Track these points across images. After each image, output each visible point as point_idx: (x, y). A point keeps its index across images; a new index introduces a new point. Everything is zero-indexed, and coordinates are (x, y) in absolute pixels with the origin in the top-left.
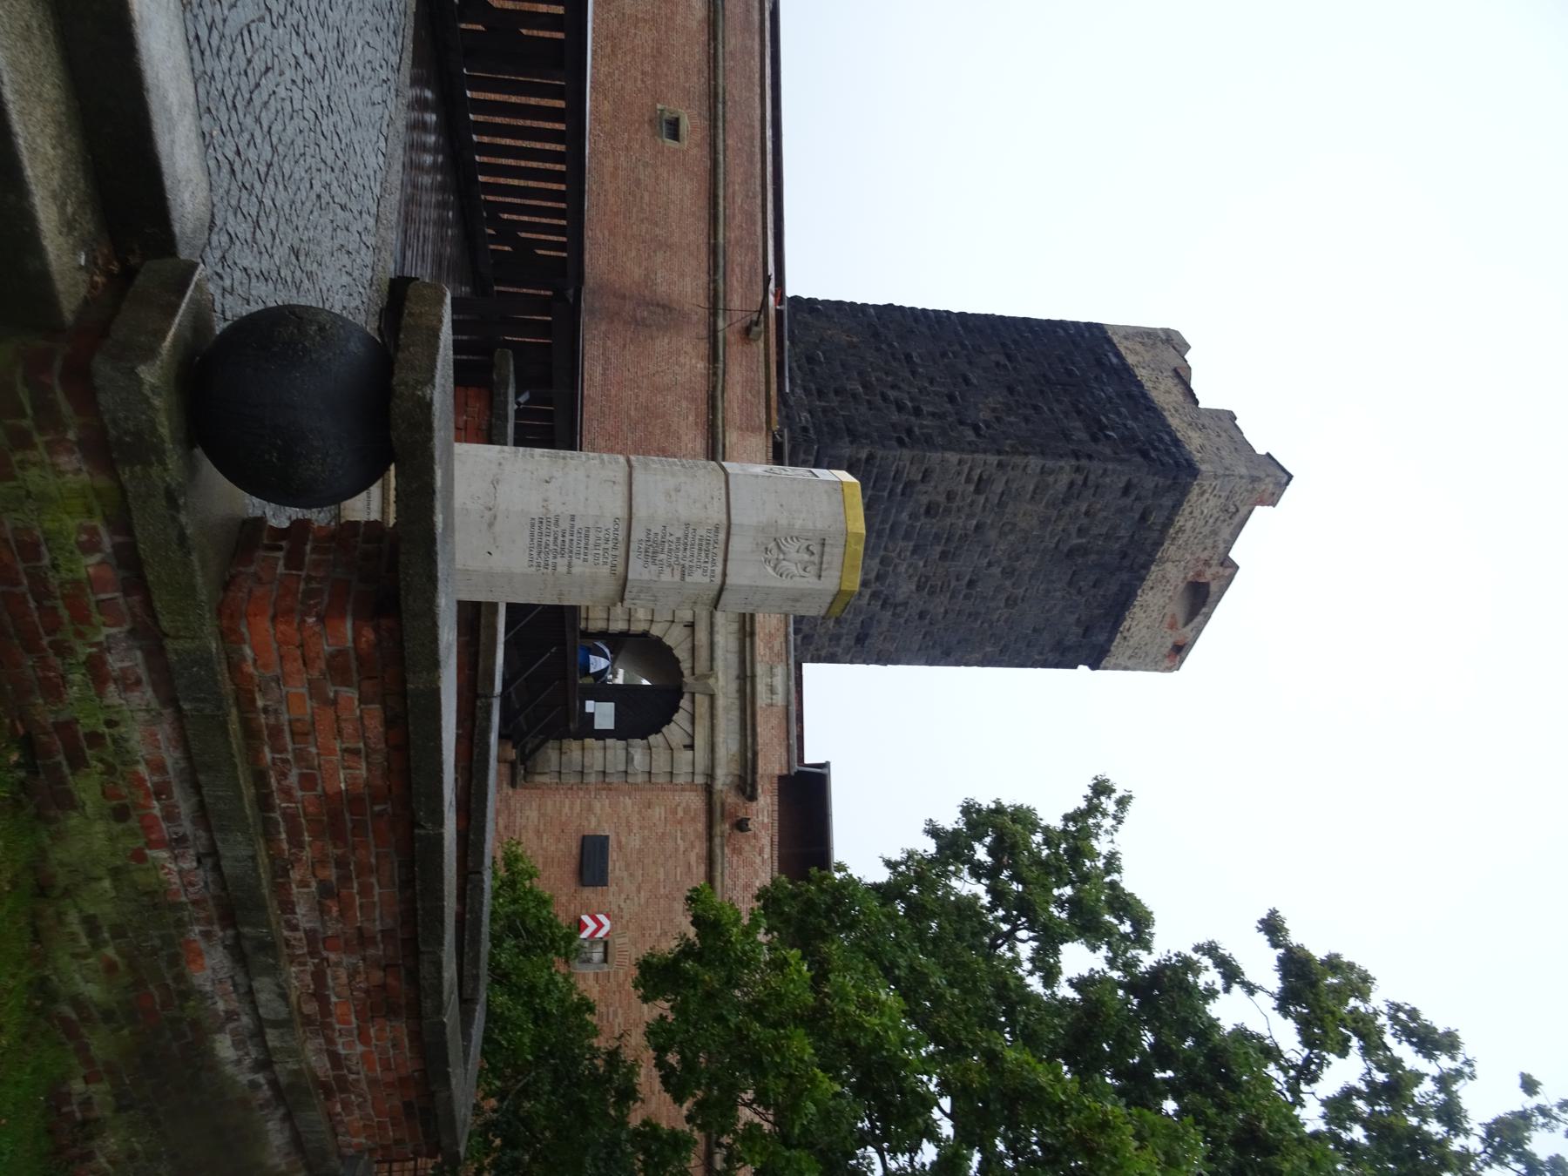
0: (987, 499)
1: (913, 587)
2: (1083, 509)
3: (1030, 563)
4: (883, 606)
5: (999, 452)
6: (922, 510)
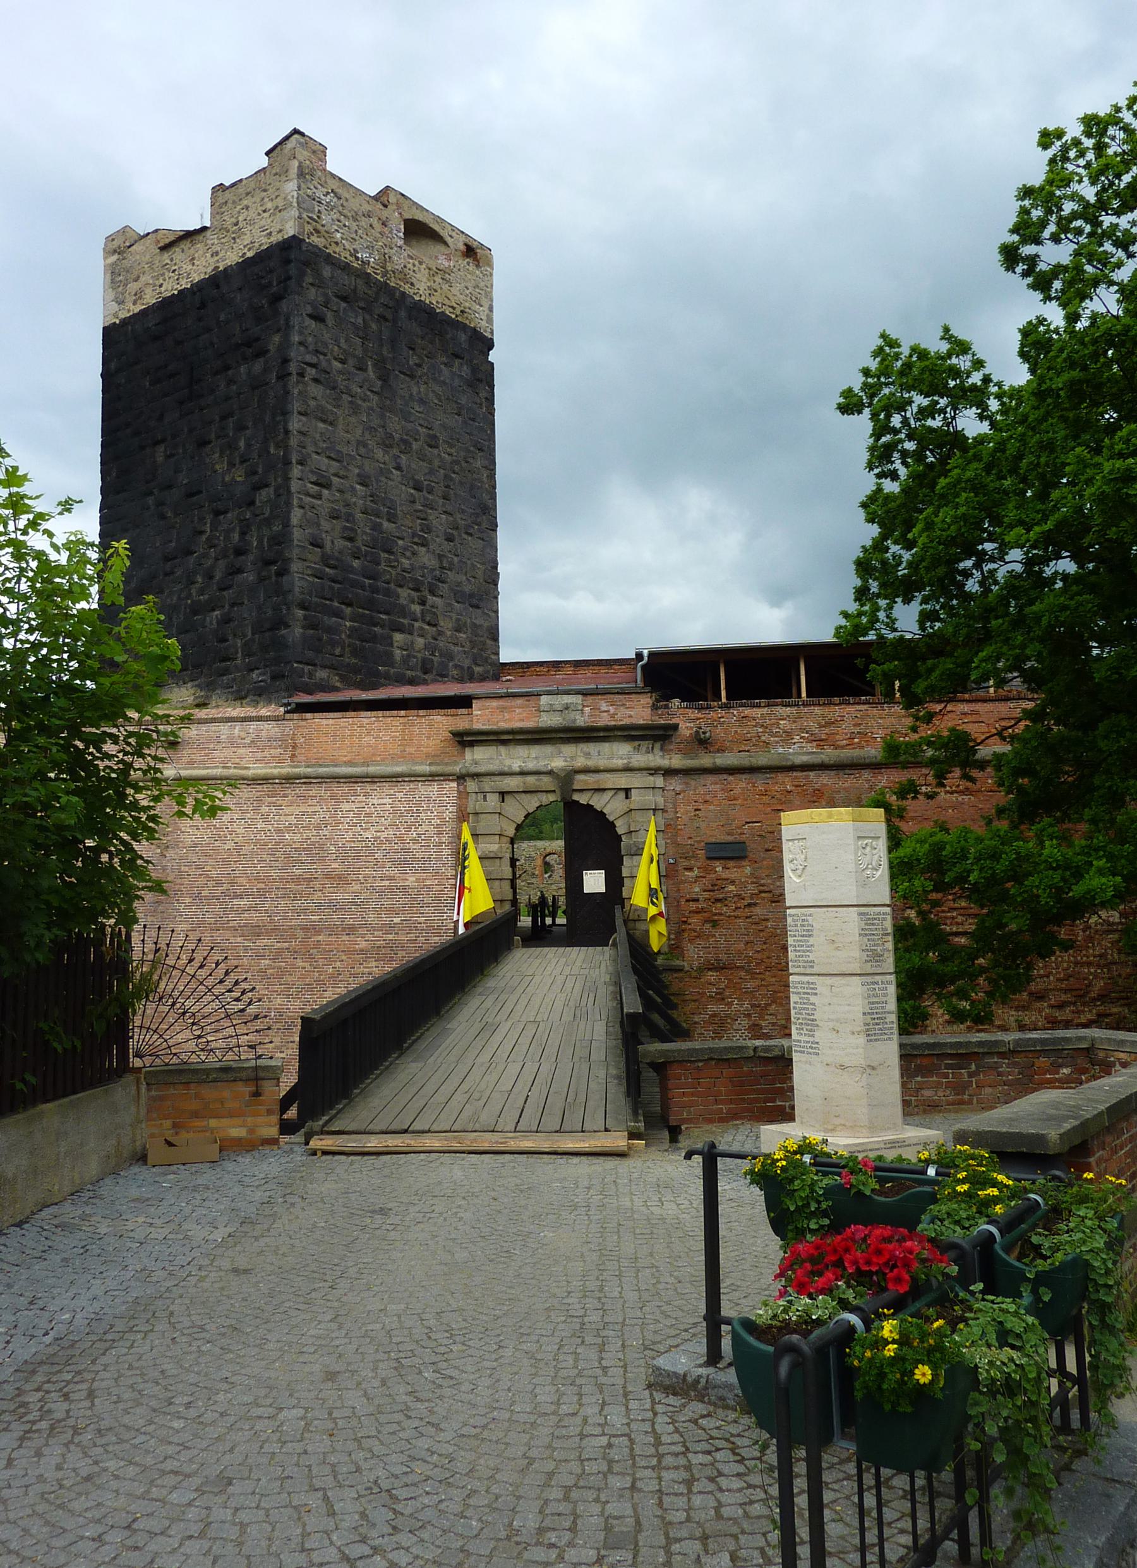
0: (336, 475)
1: (424, 549)
2: (339, 365)
3: (395, 425)
4: (442, 582)
5: (287, 463)
6: (349, 545)
